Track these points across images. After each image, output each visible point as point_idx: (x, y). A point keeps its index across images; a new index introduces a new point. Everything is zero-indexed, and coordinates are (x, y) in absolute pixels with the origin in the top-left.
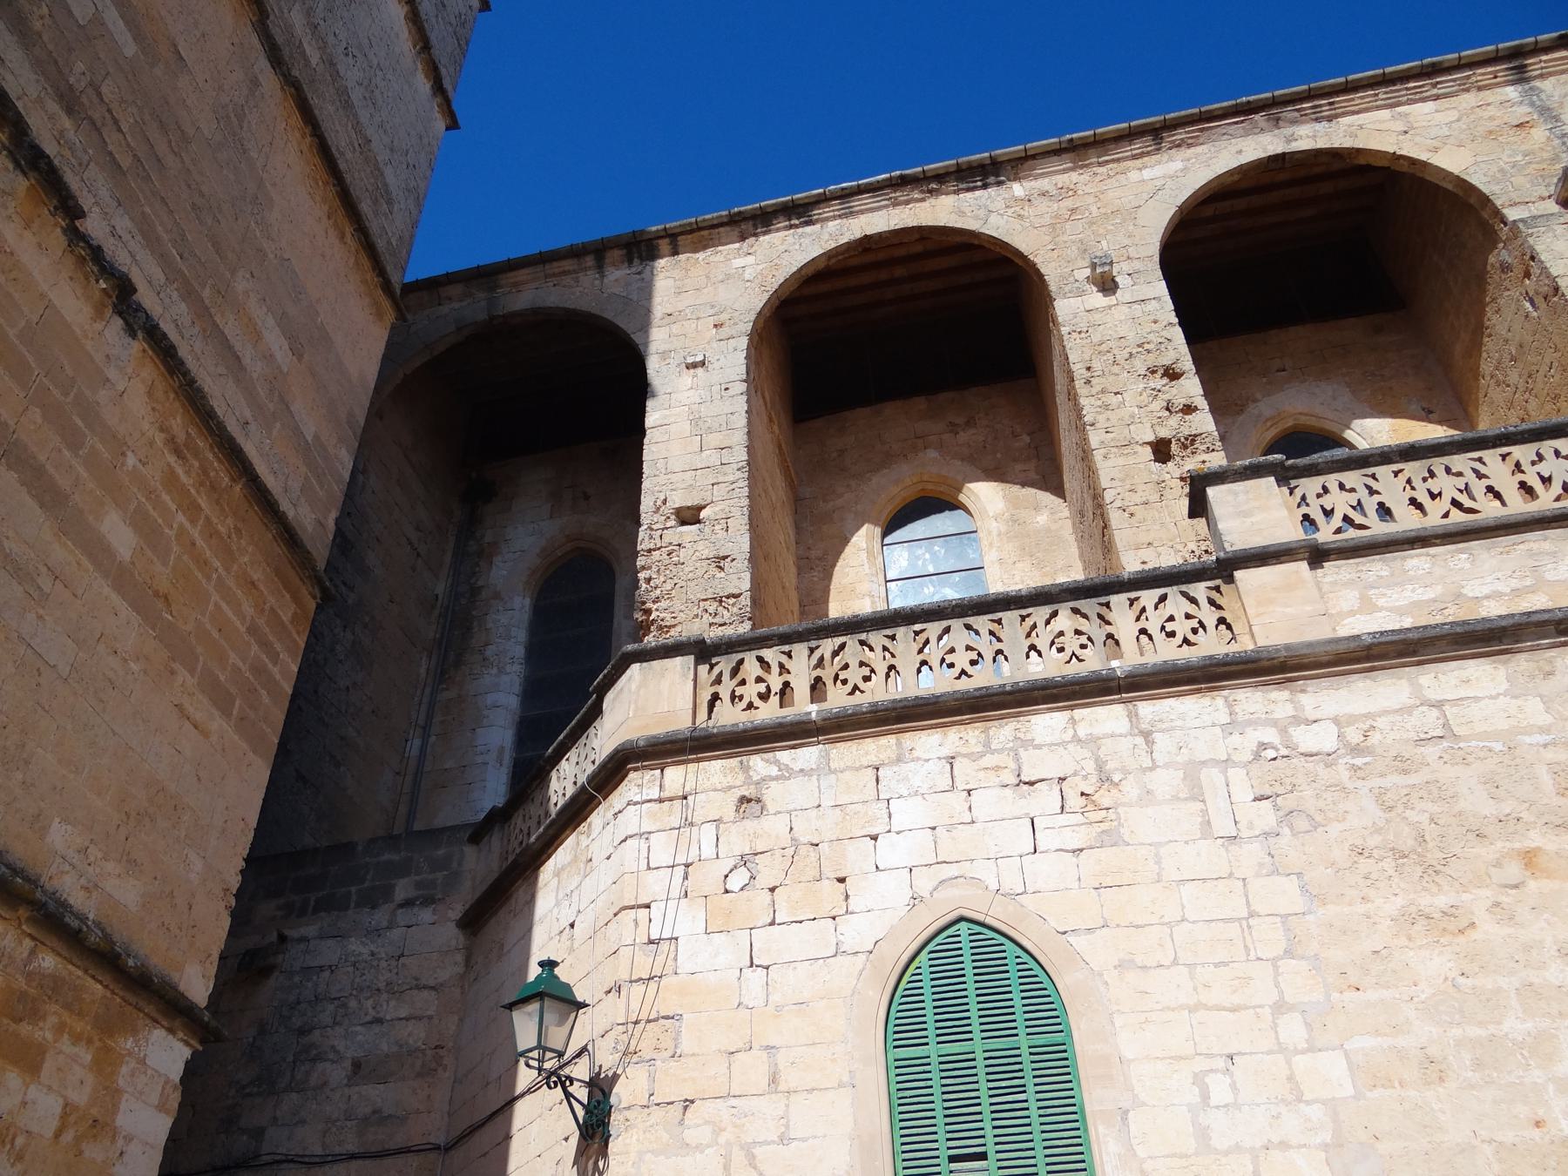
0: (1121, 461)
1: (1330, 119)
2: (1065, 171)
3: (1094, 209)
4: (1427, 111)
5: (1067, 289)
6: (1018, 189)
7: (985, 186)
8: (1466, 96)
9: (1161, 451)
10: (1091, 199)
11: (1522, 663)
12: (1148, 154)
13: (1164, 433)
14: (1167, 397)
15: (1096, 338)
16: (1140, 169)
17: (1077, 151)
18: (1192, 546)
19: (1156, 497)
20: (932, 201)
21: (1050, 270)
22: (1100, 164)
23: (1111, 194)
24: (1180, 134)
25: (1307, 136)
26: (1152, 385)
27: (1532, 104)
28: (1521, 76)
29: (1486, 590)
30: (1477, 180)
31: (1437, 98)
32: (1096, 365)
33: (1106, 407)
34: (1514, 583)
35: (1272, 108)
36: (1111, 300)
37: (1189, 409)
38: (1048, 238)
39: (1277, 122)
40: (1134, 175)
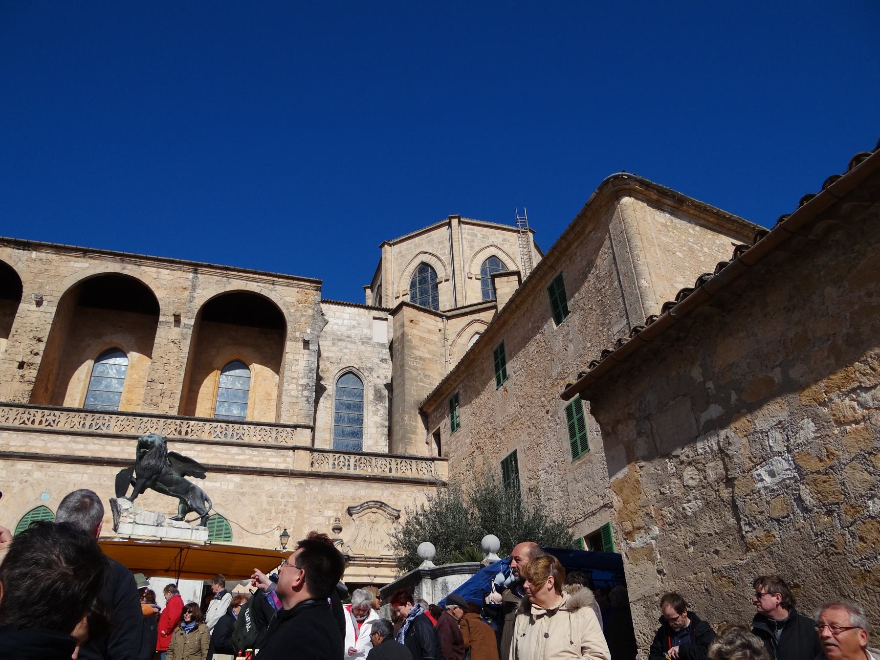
0: (8, 366)
1: (139, 265)
2: (52, 253)
3: (52, 272)
4: (166, 273)
5: (27, 300)
6: (34, 254)
7: (24, 250)
8: (179, 272)
9: (21, 365)
10: (54, 268)
11: (9, 462)
12: (81, 257)
13: (25, 360)
14: (32, 348)
15: (25, 321)
16: (75, 262)
17: (58, 249)
18: (11, 398)
19: (10, 380)
20: (4, 248)
21: (26, 291)
22: (65, 255)
23: (61, 268)
24: (92, 255)
25: (130, 270)
26: (31, 343)
27: (193, 282)
28: (196, 271)
29: (14, 444)
30: (161, 303)
31: (171, 270)
32: (19, 331)
33: (14, 346)
34: (21, 444)
35: (123, 257)
36: (37, 309)
37: (37, 354)
38: (32, 278)
39: (122, 261)
40: (72, 264)
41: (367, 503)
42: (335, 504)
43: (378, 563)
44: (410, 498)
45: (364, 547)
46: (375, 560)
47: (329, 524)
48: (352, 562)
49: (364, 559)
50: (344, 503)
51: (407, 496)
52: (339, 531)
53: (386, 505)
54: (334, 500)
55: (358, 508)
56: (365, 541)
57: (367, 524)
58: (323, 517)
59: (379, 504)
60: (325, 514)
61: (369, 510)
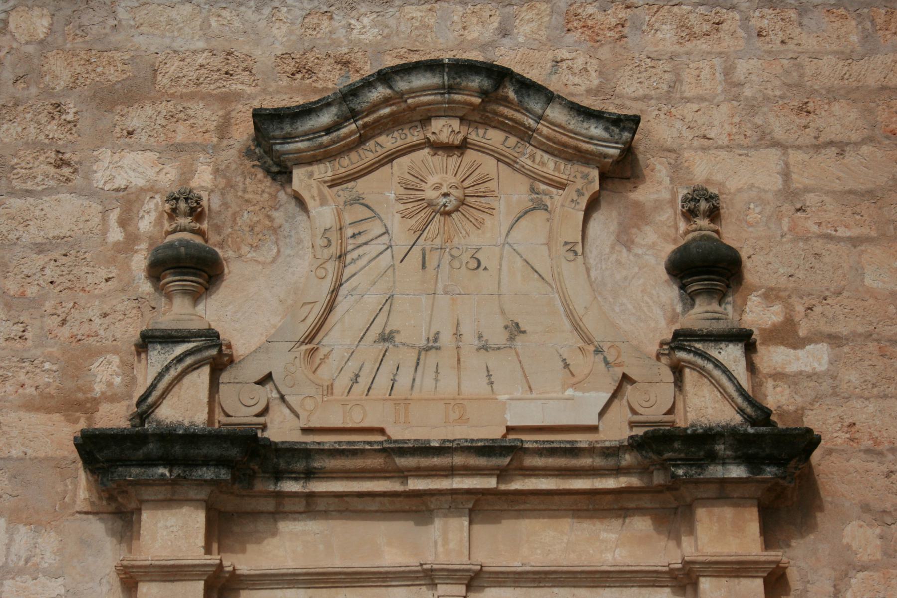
41: (385, 77)
42: (164, 107)
43: (491, 483)
44: (703, 45)
45: (383, 381)
46: (458, 460)
47: (131, 239)
48: (291, 486)
49: (376, 462)
50: (226, 99)
51: (687, 33)
52: (191, 282)
53: (526, 86)
54: (163, 81)
55: (326, 118)
56: (386, 338)
57: (396, 224)
58: (91, 193)
59: (476, 82)
60: (99, 179)
61: (415, 136)
